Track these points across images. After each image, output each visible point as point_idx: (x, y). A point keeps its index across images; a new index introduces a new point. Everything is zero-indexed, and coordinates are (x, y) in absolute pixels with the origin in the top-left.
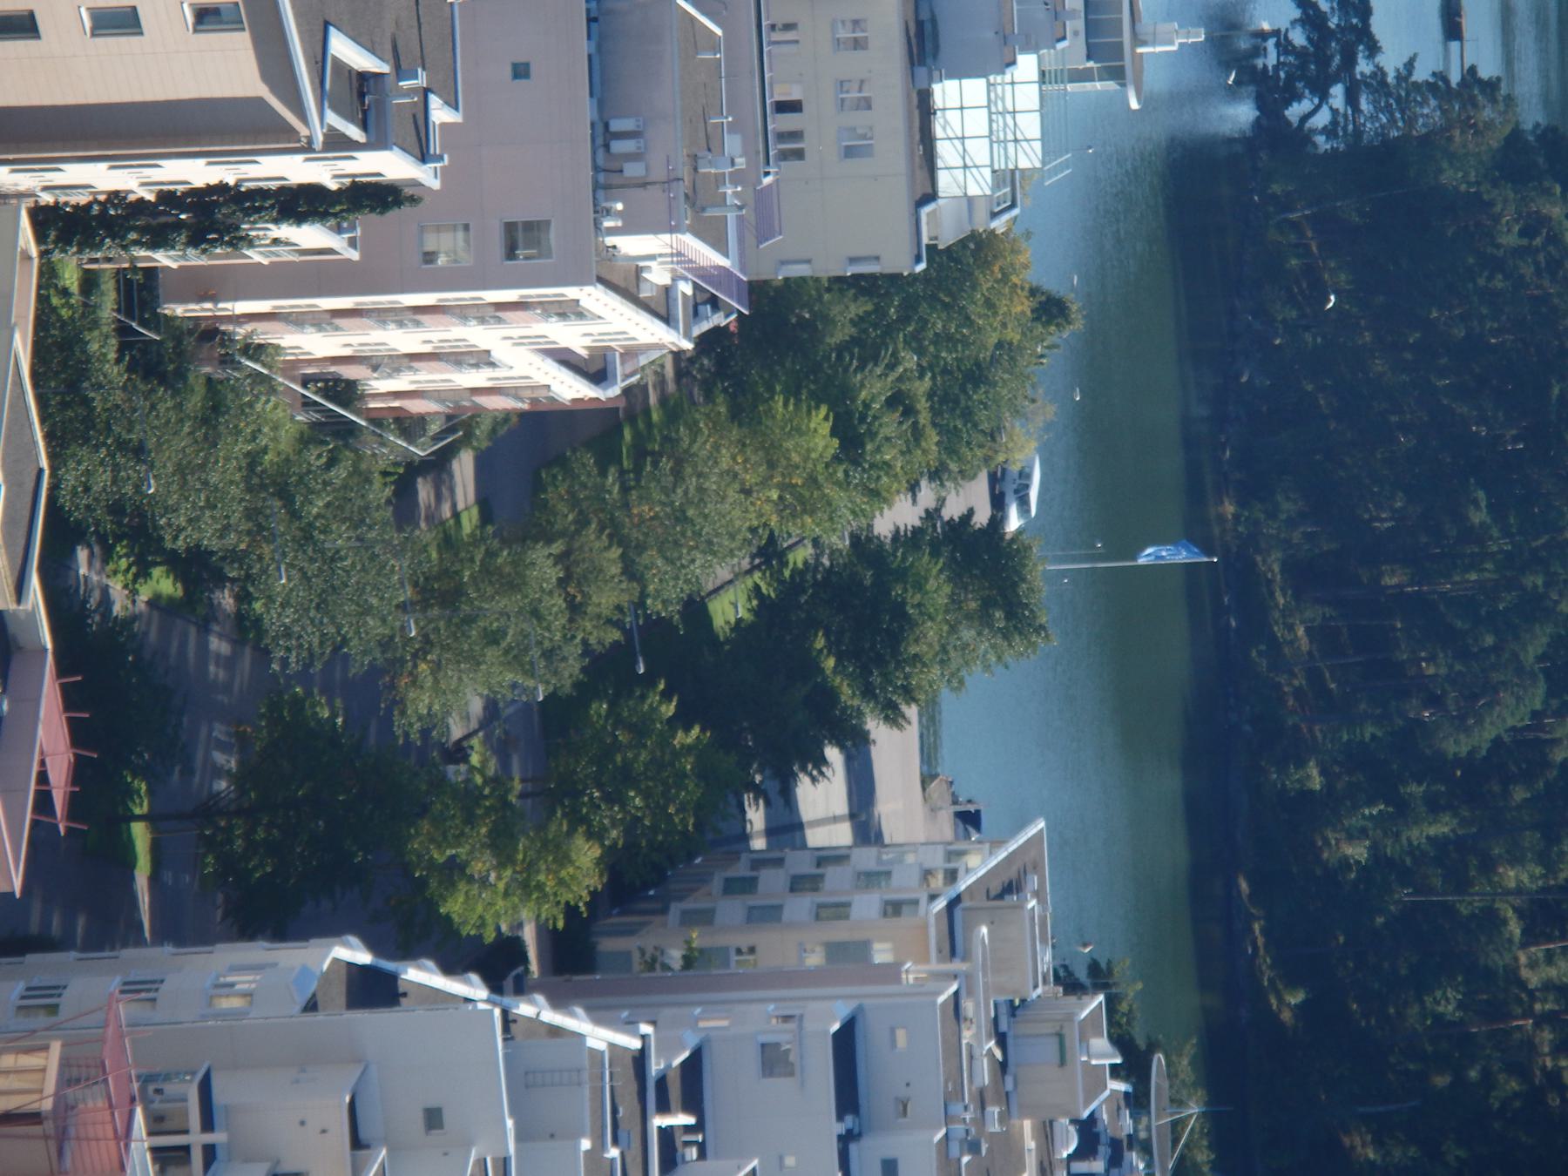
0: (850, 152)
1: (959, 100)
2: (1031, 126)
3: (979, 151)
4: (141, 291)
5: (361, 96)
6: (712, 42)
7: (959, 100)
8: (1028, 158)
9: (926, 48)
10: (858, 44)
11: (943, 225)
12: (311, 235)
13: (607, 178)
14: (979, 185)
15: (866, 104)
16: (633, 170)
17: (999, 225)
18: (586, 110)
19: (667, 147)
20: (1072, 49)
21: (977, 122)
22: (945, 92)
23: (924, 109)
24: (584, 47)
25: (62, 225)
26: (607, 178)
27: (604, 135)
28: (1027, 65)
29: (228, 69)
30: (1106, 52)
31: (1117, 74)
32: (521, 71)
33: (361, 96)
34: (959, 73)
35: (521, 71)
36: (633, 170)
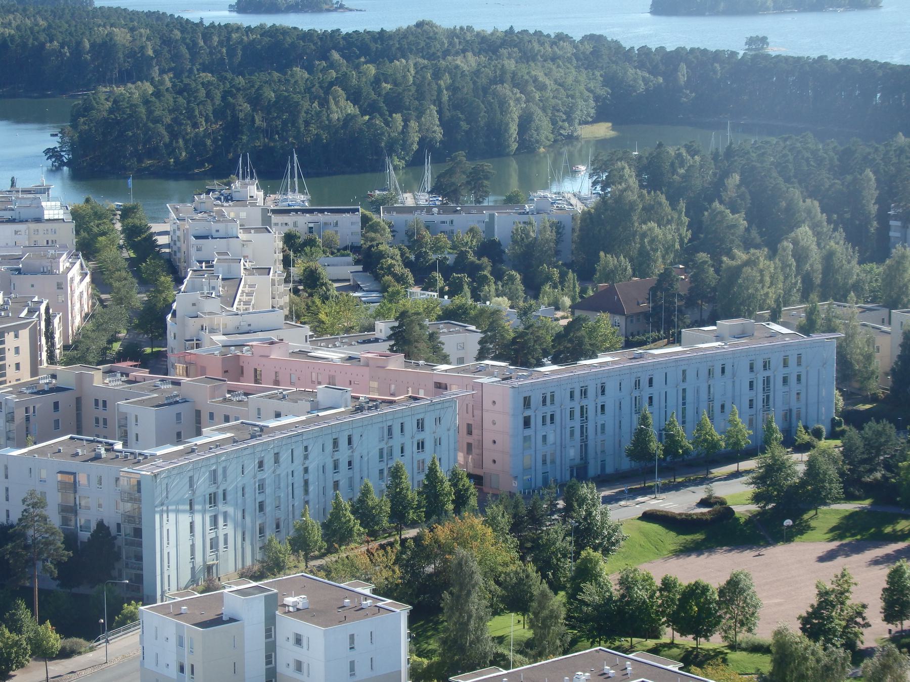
2: (53, 203)
3: (56, 212)
4: (66, 347)
5: (31, 312)
8: (58, 204)
9: (39, 220)
11: (69, 218)
12: (56, 321)
13: (48, 272)
18: (39, 276)
19: (46, 263)
21: (51, 212)
22: (46, 217)
23: (49, 220)
25: (51, 358)
26: (50, 272)
27: (43, 273)
28: (43, 204)
29: (25, 334)
30: (44, 190)
31: (48, 189)
32: (33, 286)
33: (31, 312)
35: (33, 286)
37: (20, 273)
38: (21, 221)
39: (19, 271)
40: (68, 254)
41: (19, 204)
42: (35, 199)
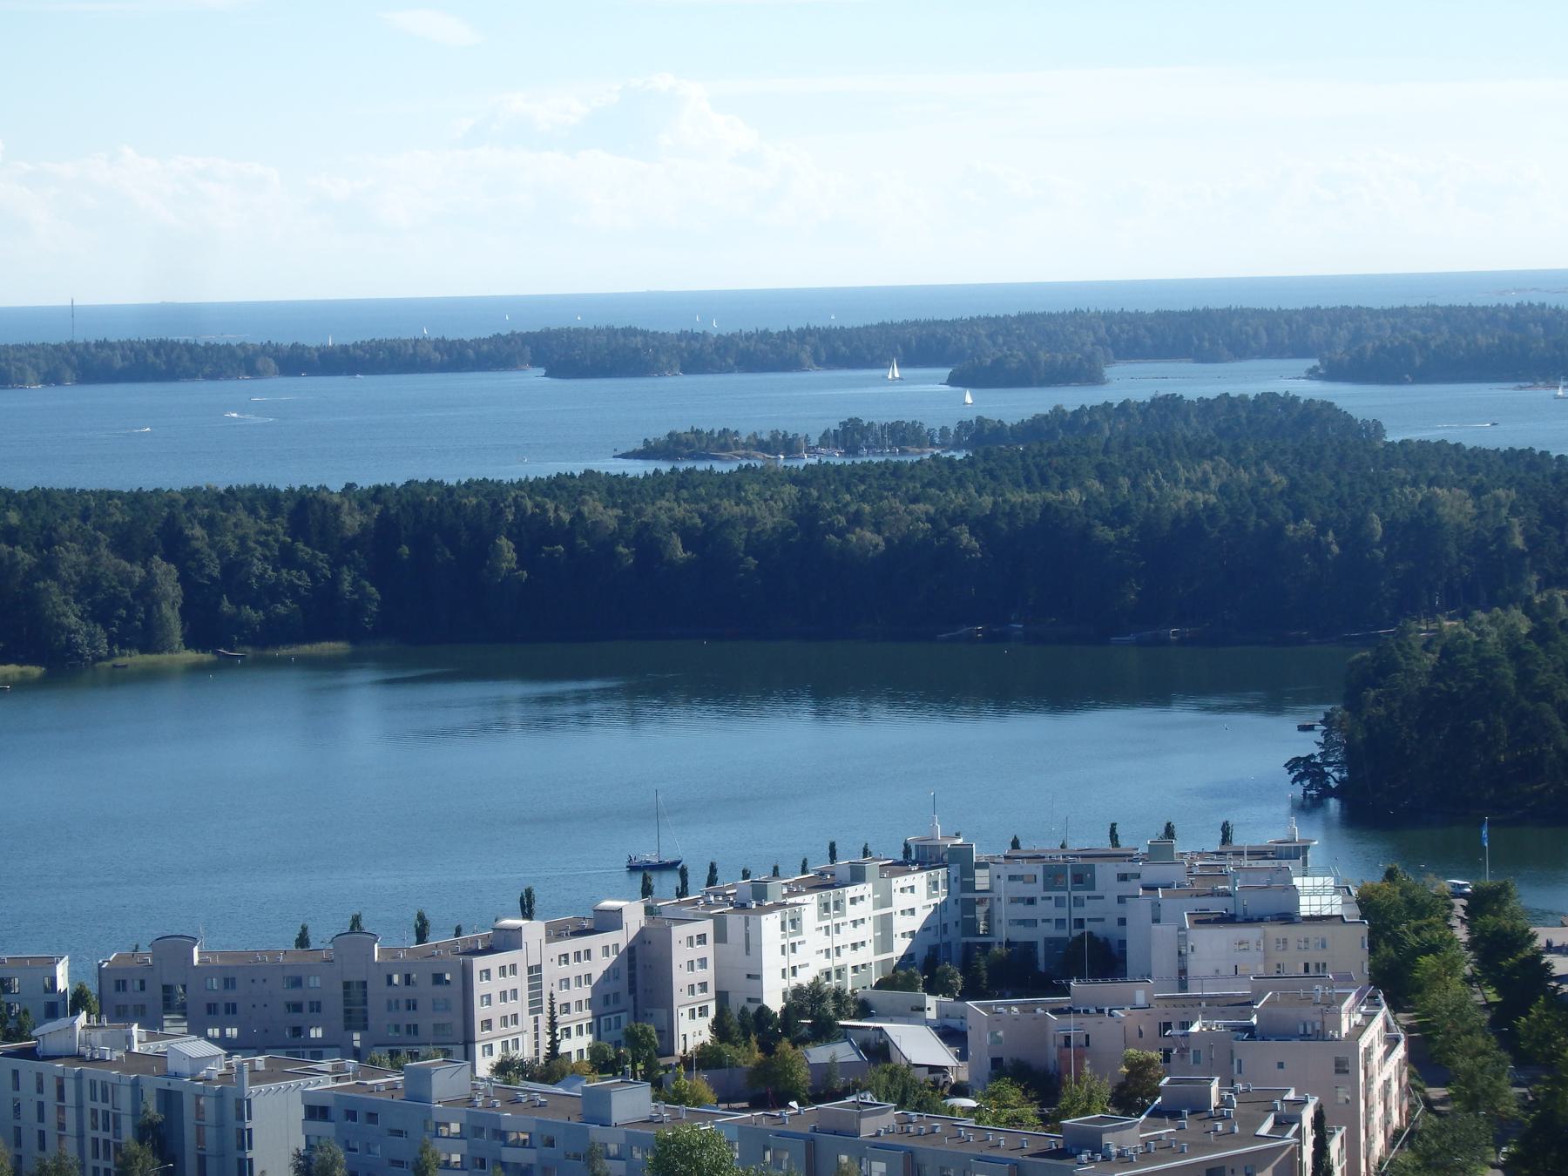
0: (1324, 946)
1: (1307, 906)
2: (1319, 881)
3: (1326, 900)
5: (1282, 1124)
6: (1274, 995)
7: (1307, 906)
8: (1330, 881)
9: (1288, 917)
10: (1285, 941)
11: (1353, 913)
13: (1320, 1035)
14: (1338, 899)
15: (1307, 941)
16: (1318, 1026)
17: (1354, 892)
18: (1295, 1042)
19: (1310, 1014)
20: (1292, 865)
22: (1304, 911)
24: (1273, 1042)
26: (1320, 1035)
27: (1305, 1036)
28: (1297, 881)
32: (1281, 1065)
33: (1282, 1124)
34: (1298, 905)
35: (1281, 1065)
36: (1318, 1026)
37: (1252, 1037)
38: (1249, 920)
39: (1250, 1031)
40: (1359, 995)
41: (1242, 882)
42: (1279, 870)
